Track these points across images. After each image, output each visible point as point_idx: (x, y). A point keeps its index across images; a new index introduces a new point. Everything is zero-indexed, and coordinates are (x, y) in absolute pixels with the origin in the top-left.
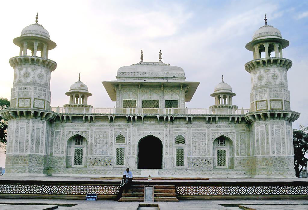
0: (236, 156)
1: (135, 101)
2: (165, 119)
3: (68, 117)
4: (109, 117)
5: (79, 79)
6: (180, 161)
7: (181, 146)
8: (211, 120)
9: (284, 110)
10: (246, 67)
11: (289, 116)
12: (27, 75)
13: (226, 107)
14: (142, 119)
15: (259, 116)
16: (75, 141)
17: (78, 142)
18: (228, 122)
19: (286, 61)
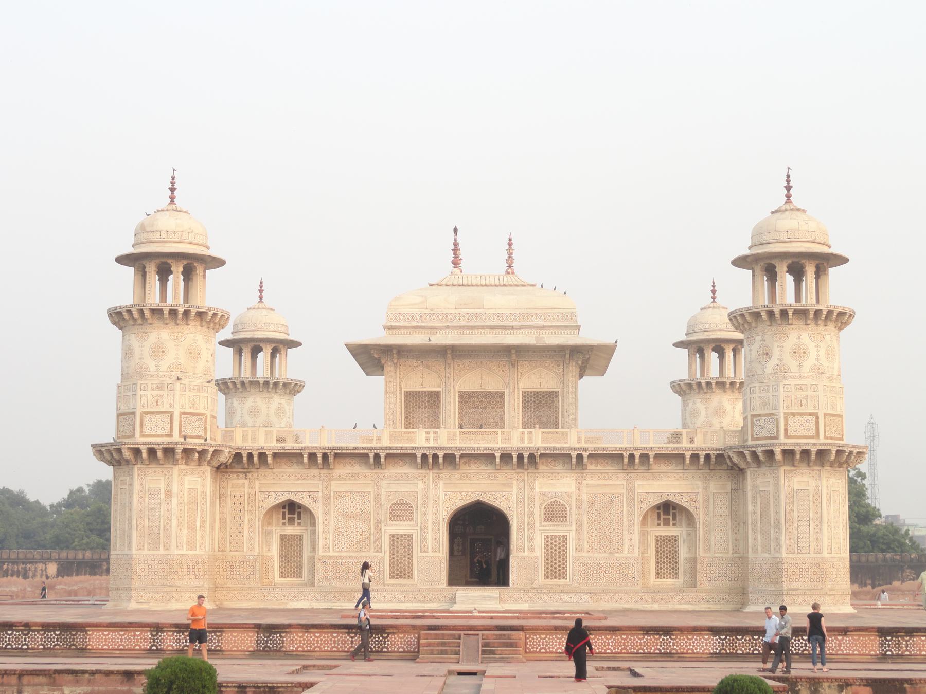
0: (701, 553)
1: (437, 394)
2: (515, 459)
3: (262, 456)
4: (372, 455)
5: (261, 297)
6: (555, 566)
7: (556, 530)
8: (637, 460)
9: (822, 440)
10: (730, 320)
11: (833, 457)
12: (159, 351)
13: (721, 385)
14: (458, 460)
15: (754, 454)
16: (281, 516)
17: (289, 518)
18: (680, 467)
19: (830, 312)
